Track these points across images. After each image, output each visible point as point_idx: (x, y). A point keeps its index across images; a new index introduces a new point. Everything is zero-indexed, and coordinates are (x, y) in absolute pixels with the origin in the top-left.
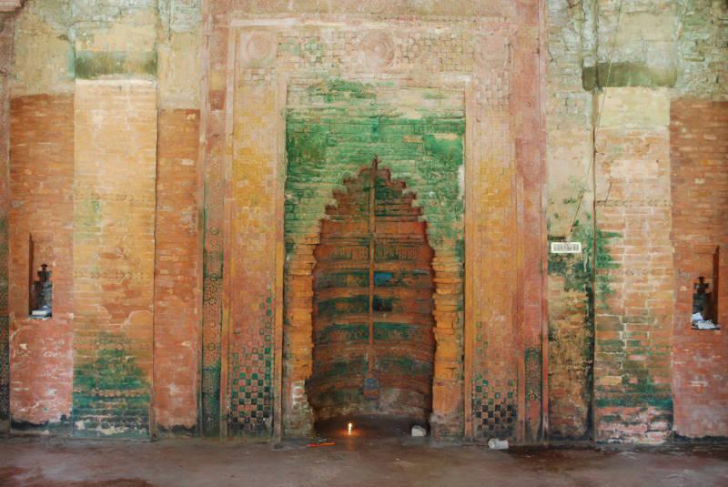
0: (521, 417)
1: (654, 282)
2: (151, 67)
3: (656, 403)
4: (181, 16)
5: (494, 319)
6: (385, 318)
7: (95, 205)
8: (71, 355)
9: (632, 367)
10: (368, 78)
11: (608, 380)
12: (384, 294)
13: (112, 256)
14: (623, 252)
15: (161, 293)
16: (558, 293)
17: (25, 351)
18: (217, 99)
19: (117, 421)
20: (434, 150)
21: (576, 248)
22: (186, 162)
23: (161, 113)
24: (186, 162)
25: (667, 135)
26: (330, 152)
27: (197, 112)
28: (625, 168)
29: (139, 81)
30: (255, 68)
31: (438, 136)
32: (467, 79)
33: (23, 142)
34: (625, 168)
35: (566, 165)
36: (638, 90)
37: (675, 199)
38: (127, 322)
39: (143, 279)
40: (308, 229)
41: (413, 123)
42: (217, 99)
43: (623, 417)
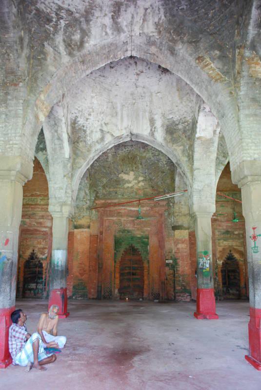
0: (161, 295)
1: (186, 268)
2: (89, 227)
3: (188, 293)
4: (95, 217)
5: (156, 276)
6: (135, 277)
7: (78, 254)
8: (72, 283)
9: (183, 285)
10: (130, 229)
11: (178, 288)
12: (134, 271)
13: (81, 264)
14: (180, 262)
15: (90, 271)
16: (168, 270)
18: (101, 233)
19: (81, 297)
20: (143, 243)
21: (171, 261)
22: (95, 245)
23: (91, 236)
24: (95, 245)
25: (188, 239)
26: (123, 243)
27: (98, 235)
28: (180, 246)
29: (86, 230)
30: (108, 226)
31: (144, 240)
32: (149, 229)
34: (180, 246)
35: (169, 245)
36: (182, 231)
37: (190, 251)
38: (83, 277)
39: (87, 268)
40: (119, 259)
41: (139, 237)
42: (101, 233)
43: (182, 295)
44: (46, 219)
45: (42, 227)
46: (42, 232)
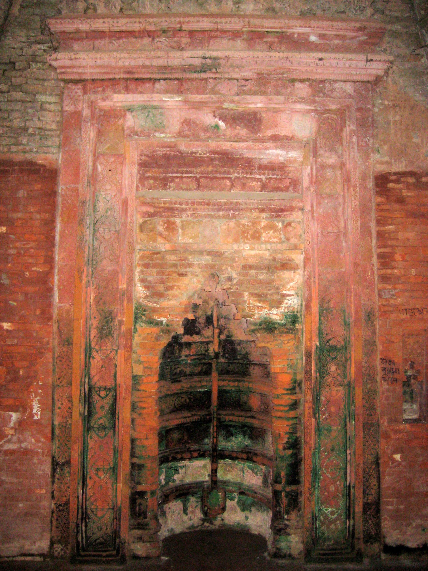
17: (399, 464)
33: (391, 224)
44: (278, 94)
45: (262, 140)
46: (262, 168)
